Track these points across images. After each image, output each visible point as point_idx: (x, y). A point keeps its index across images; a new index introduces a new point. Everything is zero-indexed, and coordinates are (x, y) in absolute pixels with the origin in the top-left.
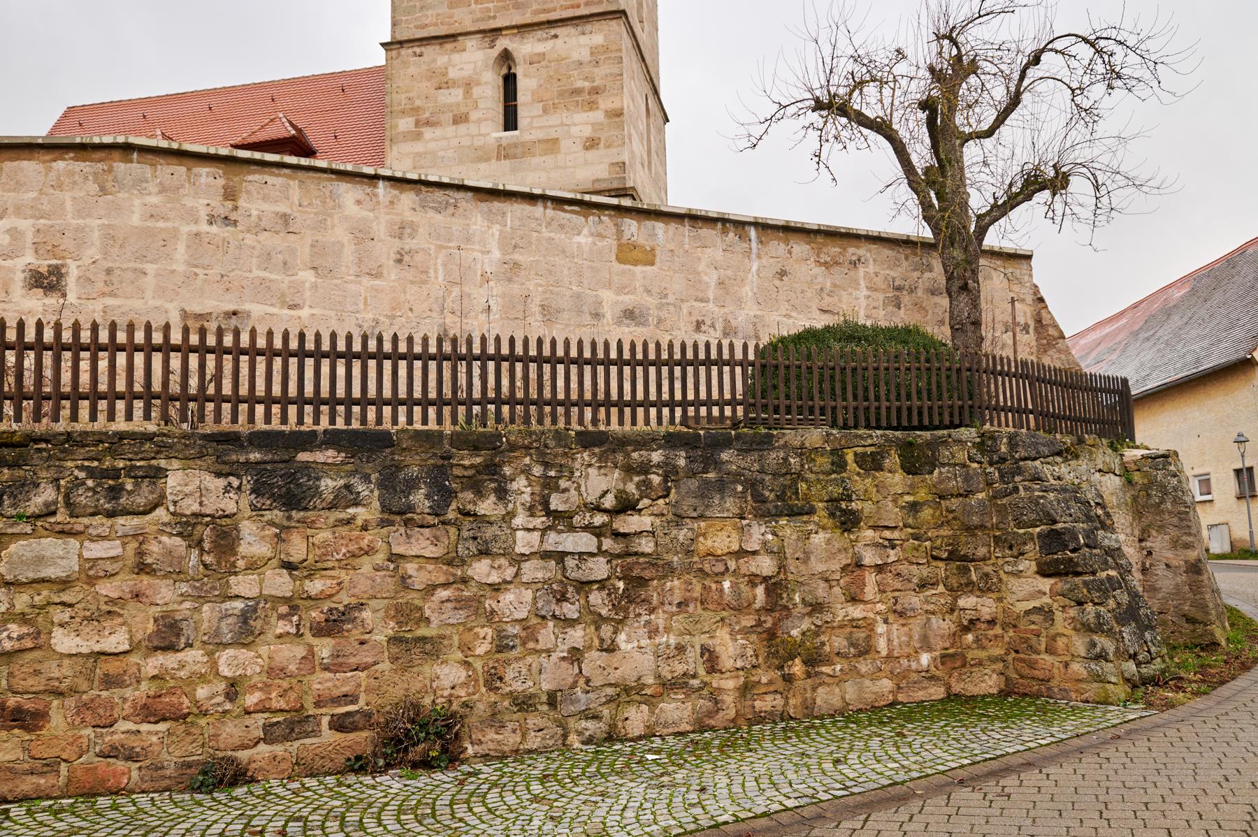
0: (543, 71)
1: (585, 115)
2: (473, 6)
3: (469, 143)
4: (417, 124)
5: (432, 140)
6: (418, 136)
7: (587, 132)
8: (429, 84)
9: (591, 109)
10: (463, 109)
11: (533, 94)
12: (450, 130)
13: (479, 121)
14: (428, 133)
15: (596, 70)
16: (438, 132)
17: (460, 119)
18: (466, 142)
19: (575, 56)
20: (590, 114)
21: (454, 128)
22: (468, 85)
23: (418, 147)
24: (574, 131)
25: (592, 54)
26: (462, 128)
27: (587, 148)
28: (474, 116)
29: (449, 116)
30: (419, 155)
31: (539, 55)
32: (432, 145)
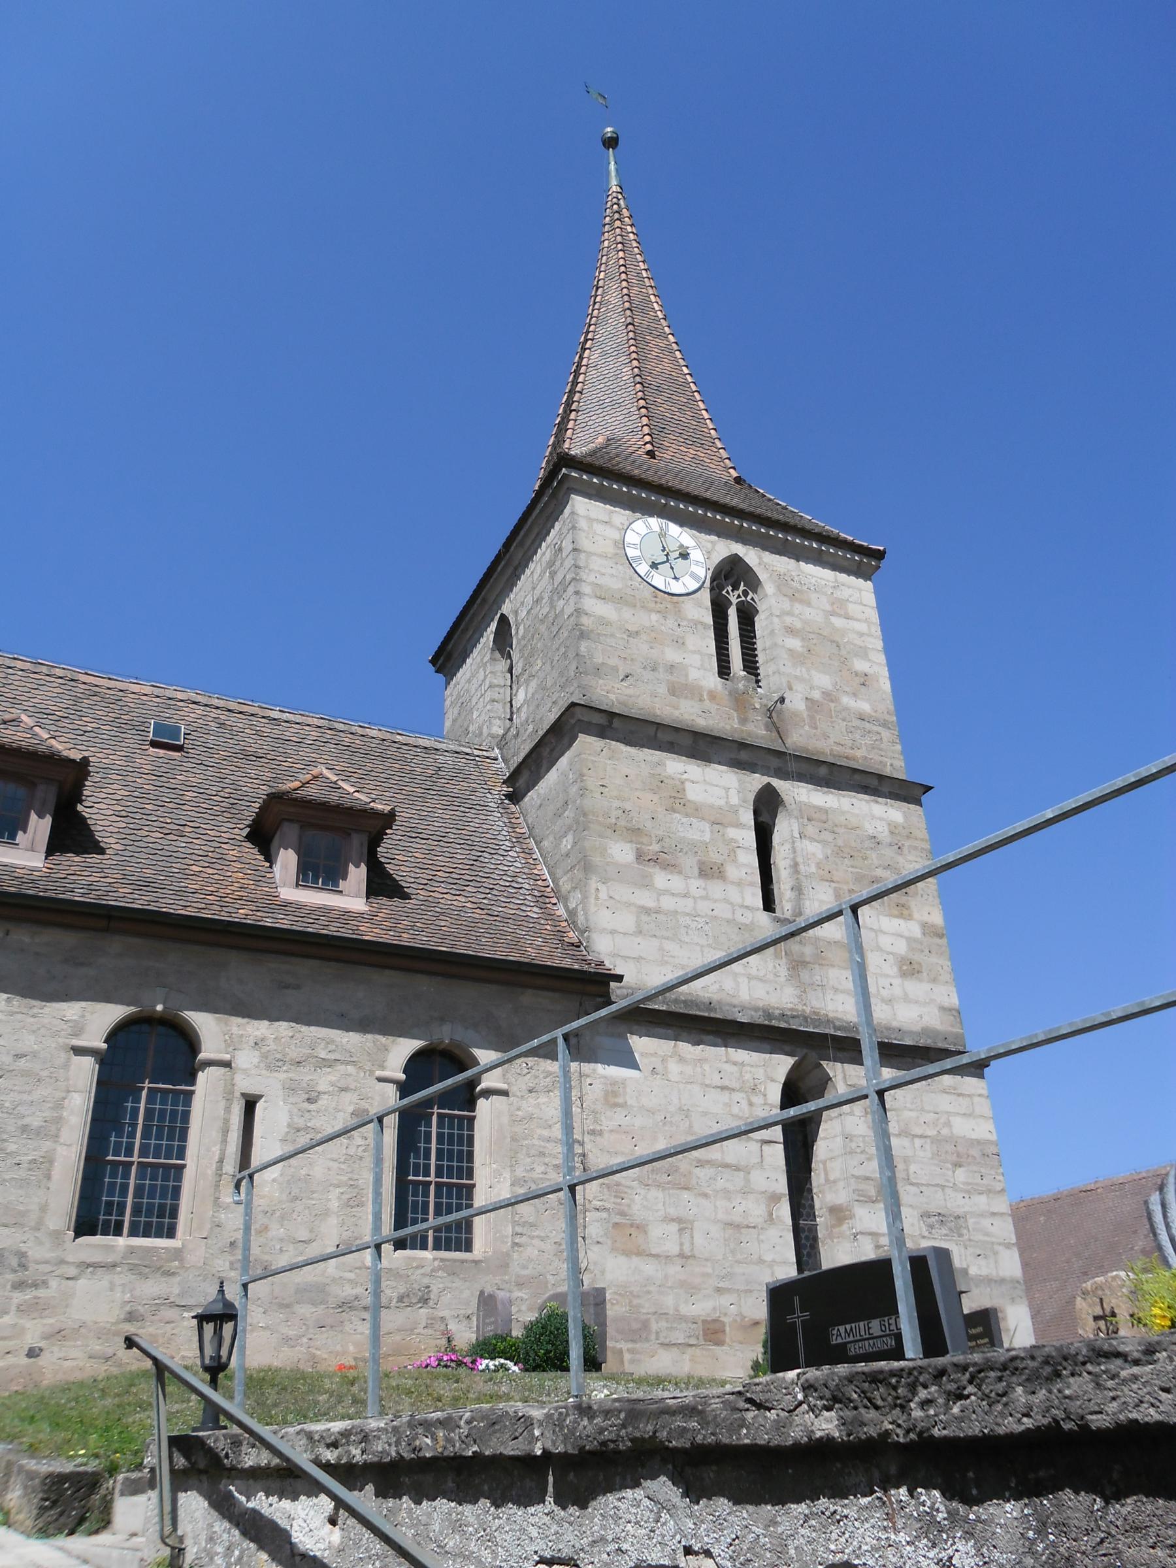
0: (828, 836)
1: (896, 921)
2: (707, 702)
3: (729, 916)
4: (639, 856)
5: (666, 892)
6: (646, 883)
7: (901, 948)
8: (656, 798)
9: (901, 916)
10: (714, 857)
11: (818, 866)
12: (695, 884)
13: (739, 884)
14: (661, 879)
15: (901, 859)
16: (676, 883)
17: (710, 871)
18: (723, 911)
19: (869, 828)
20: (901, 921)
21: (700, 882)
22: (720, 821)
23: (645, 899)
24: (885, 941)
25: (892, 833)
26: (716, 888)
27: (904, 975)
28: (732, 872)
29: (689, 863)
30: (647, 911)
31: (819, 809)
32: (667, 903)
